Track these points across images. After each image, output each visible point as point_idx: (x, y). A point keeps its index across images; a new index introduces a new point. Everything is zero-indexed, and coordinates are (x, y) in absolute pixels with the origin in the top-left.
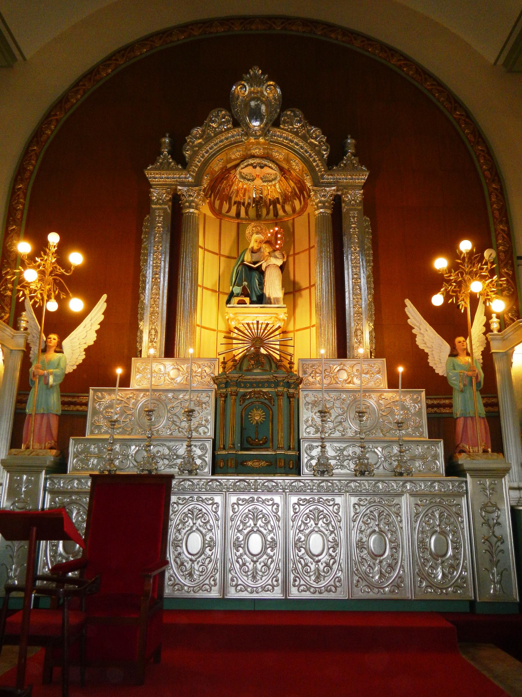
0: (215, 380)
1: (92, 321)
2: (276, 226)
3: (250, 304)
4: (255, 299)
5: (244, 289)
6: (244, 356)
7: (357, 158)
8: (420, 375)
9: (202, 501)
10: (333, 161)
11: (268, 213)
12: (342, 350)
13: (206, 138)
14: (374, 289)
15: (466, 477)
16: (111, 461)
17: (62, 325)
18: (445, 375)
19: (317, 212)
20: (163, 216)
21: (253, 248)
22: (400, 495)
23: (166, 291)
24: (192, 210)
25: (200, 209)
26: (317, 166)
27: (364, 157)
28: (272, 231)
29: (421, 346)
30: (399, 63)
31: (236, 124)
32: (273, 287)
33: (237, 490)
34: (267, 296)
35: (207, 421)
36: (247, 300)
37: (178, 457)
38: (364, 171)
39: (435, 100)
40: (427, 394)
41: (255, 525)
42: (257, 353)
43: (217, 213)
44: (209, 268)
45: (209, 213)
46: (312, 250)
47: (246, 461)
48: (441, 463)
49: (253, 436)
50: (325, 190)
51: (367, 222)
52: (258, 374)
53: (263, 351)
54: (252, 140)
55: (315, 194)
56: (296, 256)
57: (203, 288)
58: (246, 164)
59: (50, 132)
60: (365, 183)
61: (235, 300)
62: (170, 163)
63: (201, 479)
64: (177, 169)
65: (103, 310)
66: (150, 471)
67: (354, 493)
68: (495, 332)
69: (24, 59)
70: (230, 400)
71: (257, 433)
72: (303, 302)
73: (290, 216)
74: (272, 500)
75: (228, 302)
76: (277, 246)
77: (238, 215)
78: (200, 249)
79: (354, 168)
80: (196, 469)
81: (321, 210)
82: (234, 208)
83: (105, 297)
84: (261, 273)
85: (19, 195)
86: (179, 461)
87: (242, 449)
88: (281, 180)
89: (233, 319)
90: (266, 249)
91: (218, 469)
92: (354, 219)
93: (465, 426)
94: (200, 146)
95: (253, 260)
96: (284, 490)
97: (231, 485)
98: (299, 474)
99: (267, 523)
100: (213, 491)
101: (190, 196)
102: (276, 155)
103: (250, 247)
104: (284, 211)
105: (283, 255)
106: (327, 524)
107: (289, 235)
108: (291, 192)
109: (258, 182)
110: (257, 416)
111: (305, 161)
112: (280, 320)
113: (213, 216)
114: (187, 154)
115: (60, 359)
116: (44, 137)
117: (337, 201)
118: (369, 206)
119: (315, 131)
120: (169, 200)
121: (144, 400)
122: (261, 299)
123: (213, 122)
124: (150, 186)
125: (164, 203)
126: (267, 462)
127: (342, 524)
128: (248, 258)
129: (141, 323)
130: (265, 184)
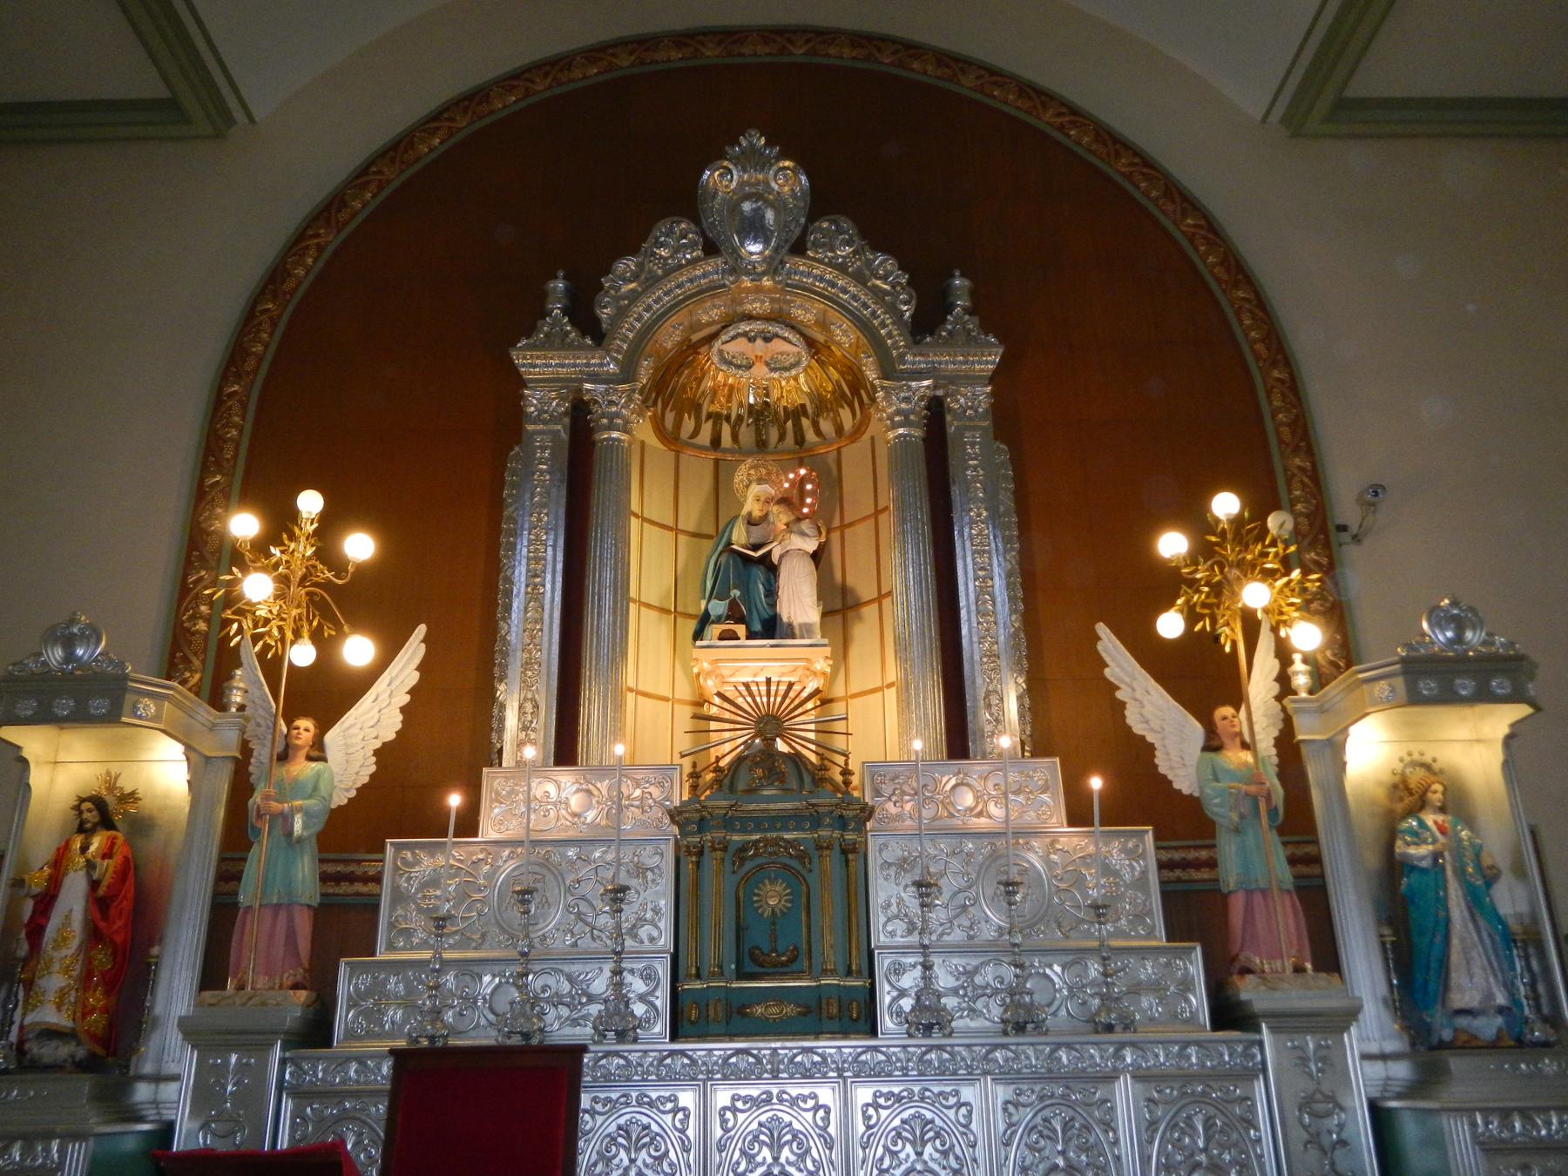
0: (675, 815)
1: (393, 686)
2: (801, 465)
3: (748, 638)
4: (757, 627)
5: (733, 605)
6: (739, 760)
7: (976, 319)
8: (1142, 797)
9: (651, 1104)
10: (925, 325)
11: (782, 437)
12: (959, 740)
13: (647, 279)
14: (1024, 600)
15: (1259, 1031)
16: (437, 1013)
17: (326, 694)
18: (1196, 794)
19: (891, 435)
20: (551, 448)
21: (750, 514)
22: (1110, 1078)
23: (557, 614)
24: (615, 435)
25: (632, 430)
26: (890, 335)
27: (992, 315)
28: (791, 476)
29: (1138, 729)
30: (1059, 120)
31: (711, 249)
32: (799, 600)
33: (730, 1073)
34: (785, 619)
35: (656, 911)
36: (741, 630)
37: (592, 999)
38: (993, 345)
39: (1137, 195)
40: (1157, 838)
41: (776, 1159)
42: (769, 753)
43: (671, 438)
44: (653, 559)
45: (652, 440)
46: (883, 518)
47: (749, 1006)
48: (1199, 1001)
49: (766, 947)
50: (909, 387)
51: (1002, 454)
52: (771, 800)
53: (781, 746)
54: (747, 282)
55: (887, 397)
56: (847, 531)
57: (641, 604)
58: (732, 333)
59: (304, 272)
60: (995, 372)
61: (715, 630)
62: (567, 333)
63: (646, 1052)
64: (581, 347)
65: (417, 661)
66: (526, 1036)
67: (1004, 1076)
68: (1304, 695)
69: (252, 120)
70: (711, 861)
71: (774, 937)
72: (864, 632)
73: (831, 445)
74: (814, 1096)
75: (698, 635)
76: (805, 510)
77: (716, 442)
78: (633, 519)
79: (970, 340)
80: (634, 1028)
81: (901, 431)
82: (707, 428)
83: (421, 630)
84: (771, 568)
85: (230, 408)
86: (595, 1009)
87: (741, 975)
88: (809, 366)
89: (709, 674)
90: (781, 517)
91: (685, 1027)
92: (973, 447)
93: (1249, 909)
94: (634, 297)
95: (752, 541)
96: (840, 1072)
97: (716, 1063)
98: (873, 1033)
99: (804, 1154)
100: (673, 1078)
101: (611, 403)
102: (798, 313)
103: (744, 512)
104: (818, 432)
105: (819, 528)
106: (945, 1154)
107: (831, 483)
108: (833, 392)
109: (760, 371)
110: (773, 897)
111: (863, 325)
112: (815, 674)
113: (661, 446)
114: (605, 313)
115: (318, 775)
116: (289, 285)
117: (935, 412)
118: (1006, 420)
119: (883, 262)
120: (565, 413)
121: (511, 865)
122: (772, 628)
123: (662, 245)
124: (523, 384)
125: (554, 420)
126: (798, 1005)
127: (979, 1152)
128: (739, 537)
129: (502, 687)
130: (776, 375)
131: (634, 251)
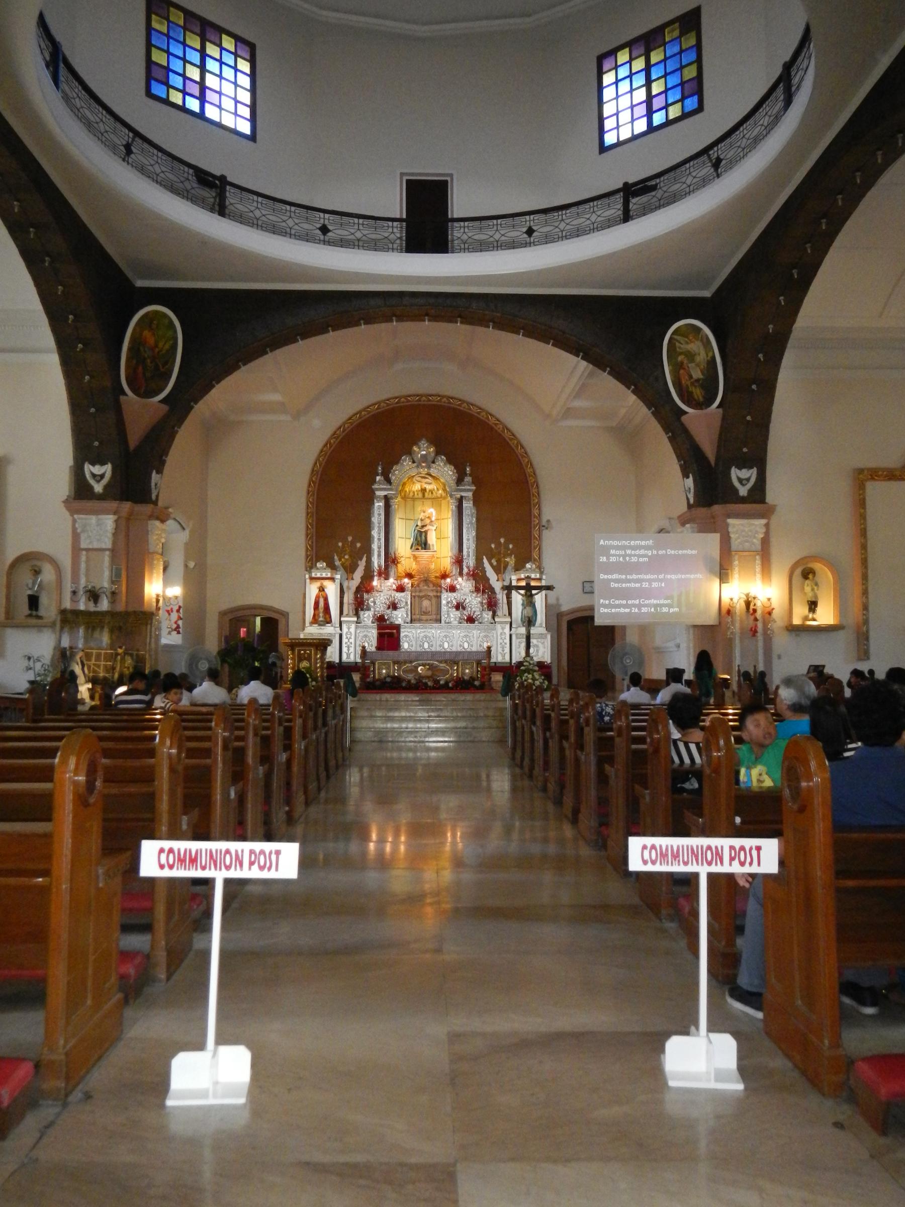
43: (405, 498)
84: (426, 532)
131: (397, 463)
